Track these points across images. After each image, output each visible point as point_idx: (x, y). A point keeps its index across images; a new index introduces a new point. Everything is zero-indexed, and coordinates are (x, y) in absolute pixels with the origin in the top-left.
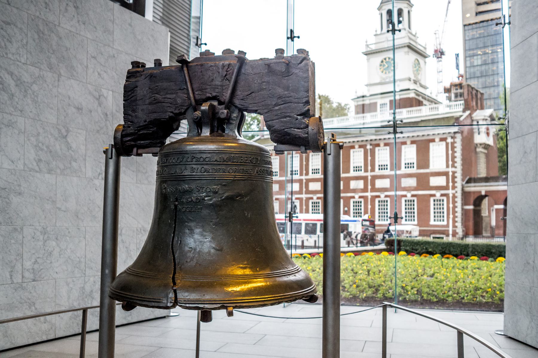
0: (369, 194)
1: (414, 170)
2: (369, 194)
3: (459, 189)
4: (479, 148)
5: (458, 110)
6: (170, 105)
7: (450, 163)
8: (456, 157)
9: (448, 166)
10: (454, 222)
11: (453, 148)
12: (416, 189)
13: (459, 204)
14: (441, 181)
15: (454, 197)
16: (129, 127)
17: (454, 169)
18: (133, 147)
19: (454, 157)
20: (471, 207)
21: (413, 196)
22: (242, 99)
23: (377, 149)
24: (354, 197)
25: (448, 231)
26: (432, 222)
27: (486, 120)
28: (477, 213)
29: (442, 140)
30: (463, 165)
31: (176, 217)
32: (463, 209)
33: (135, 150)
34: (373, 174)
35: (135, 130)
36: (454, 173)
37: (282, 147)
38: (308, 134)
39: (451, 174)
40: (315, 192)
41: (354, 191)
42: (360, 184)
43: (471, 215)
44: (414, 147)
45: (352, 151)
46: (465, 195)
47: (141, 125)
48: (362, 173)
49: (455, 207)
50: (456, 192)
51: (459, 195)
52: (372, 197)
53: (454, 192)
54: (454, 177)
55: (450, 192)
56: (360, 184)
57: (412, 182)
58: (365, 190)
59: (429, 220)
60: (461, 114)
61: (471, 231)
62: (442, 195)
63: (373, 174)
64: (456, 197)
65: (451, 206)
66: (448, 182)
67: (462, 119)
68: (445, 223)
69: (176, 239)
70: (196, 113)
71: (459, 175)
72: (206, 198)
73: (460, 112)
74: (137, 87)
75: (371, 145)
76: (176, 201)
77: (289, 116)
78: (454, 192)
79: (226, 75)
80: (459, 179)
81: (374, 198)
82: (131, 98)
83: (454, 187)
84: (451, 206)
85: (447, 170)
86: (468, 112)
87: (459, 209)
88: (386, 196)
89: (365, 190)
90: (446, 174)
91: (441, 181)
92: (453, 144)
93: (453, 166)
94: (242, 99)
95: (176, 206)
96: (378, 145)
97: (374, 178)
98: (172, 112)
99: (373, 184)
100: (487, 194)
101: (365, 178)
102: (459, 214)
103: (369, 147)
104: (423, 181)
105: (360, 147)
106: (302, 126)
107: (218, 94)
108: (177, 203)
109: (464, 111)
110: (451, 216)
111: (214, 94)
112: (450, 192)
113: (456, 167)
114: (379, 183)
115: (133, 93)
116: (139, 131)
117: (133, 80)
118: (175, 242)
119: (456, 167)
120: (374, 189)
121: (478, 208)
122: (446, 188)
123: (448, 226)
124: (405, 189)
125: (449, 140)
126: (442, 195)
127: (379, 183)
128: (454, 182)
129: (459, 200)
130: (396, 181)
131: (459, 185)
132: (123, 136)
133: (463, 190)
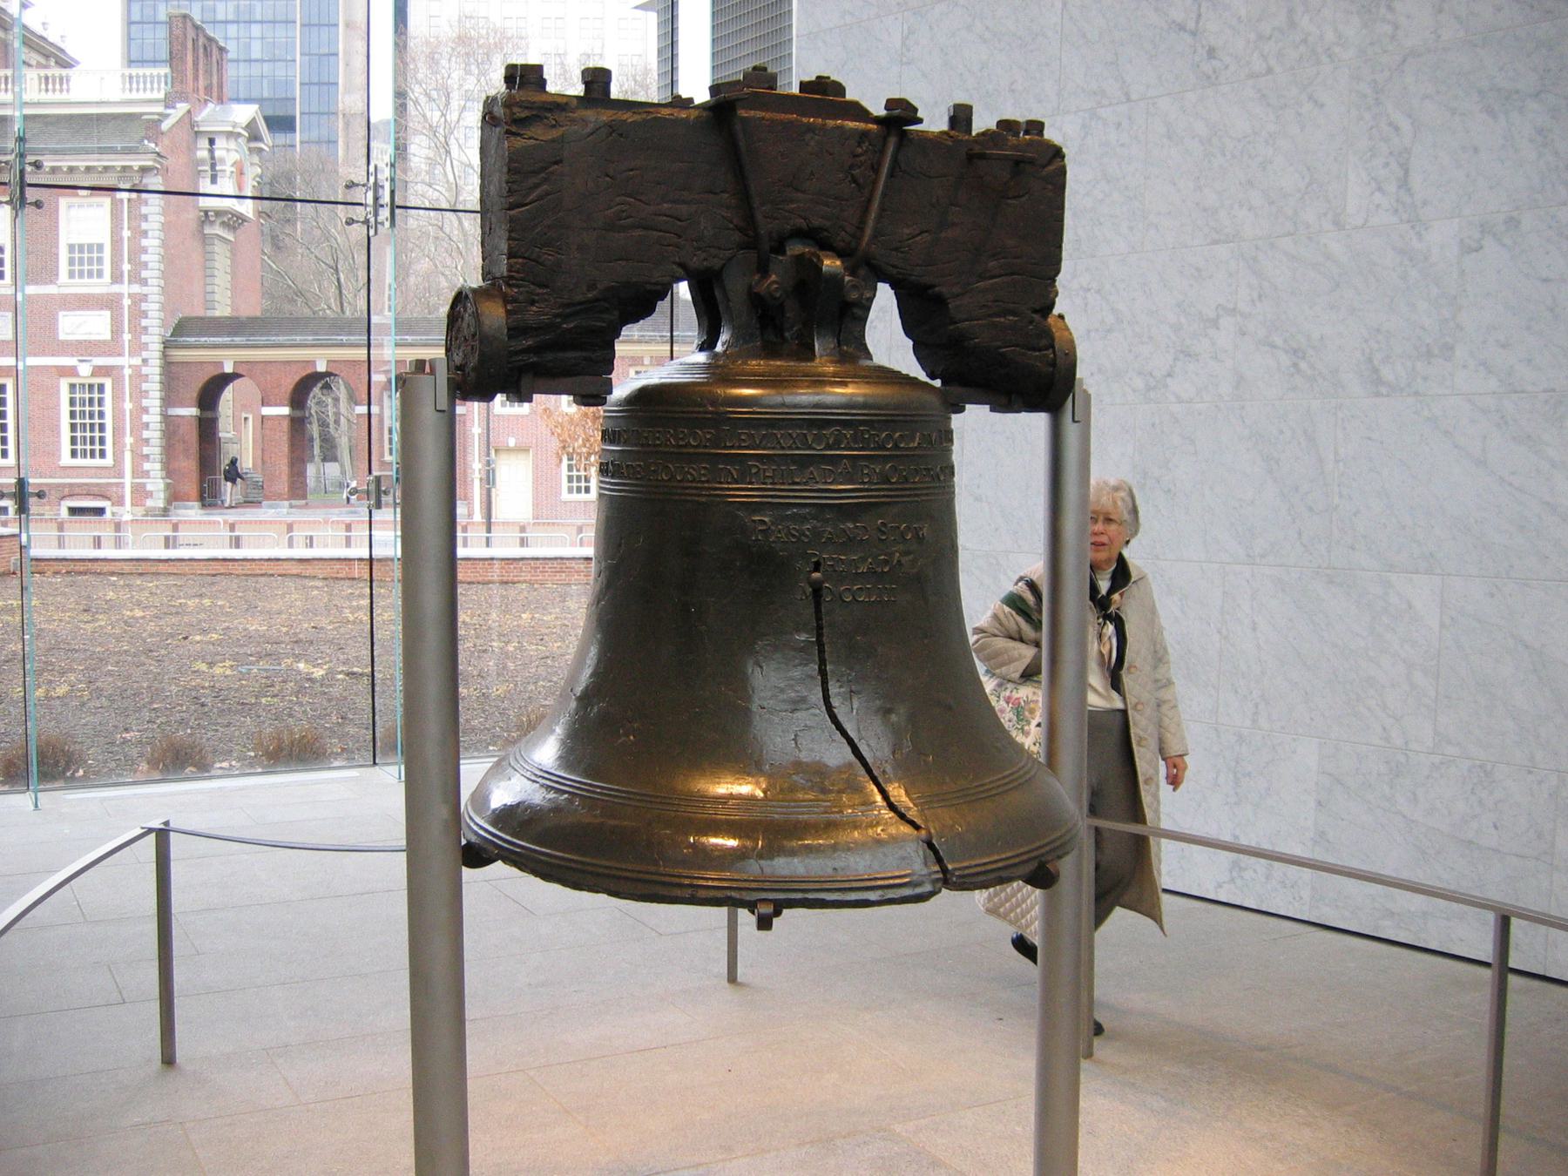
4: (212, 223)
5: (149, 95)
6: (676, 240)
7: (126, 267)
8: (145, 250)
9: (117, 278)
10: (139, 457)
13: (154, 402)
14: (96, 325)
15: (139, 377)
16: (533, 303)
17: (136, 289)
18: (522, 370)
19: (137, 251)
20: (193, 411)
22: (896, 249)
25: (121, 485)
27: (239, 135)
28: (207, 428)
30: (164, 275)
31: (819, 619)
32: (166, 418)
33: (526, 381)
35: (556, 316)
36: (138, 299)
37: (956, 390)
38: (1054, 364)
39: (127, 302)
43: (192, 436)
46: (171, 373)
47: (579, 298)
50: (145, 361)
51: (154, 370)
53: (137, 361)
54: (138, 314)
55: (125, 362)
59: (56, 453)
60: (160, 109)
61: (191, 487)
62: (98, 371)
64: (145, 378)
65: (128, 406)
66: (116, 331)
67: (165, 126)
68: (109, 461)
69: (834, 689)
70: (773, 277)
72: (904, 560)
73: (158, 101)
74: (556, 163)
76: (817, 569)
77: (1014, 313)
78: (137, 361)
79: (852, 167)
82: (540, 198)
83: (138, 348)
84: (128, 406)
85: (116, 288)
86: (182, 107)
87: (154, 418)
90: (109, 303)
91: (96, 325)
93: (136, 278)
94: (896, 249)
95: (817, 591)
98: (681, 265)
100: (240, 371)
102: (154, 434)
106: (1044, 342)
107: (828, 224)
108: (816, 575)
109: (169, 102)
110: (129, 440)
111: (817, 222)
112: (125, 362)
113: (144, 282)
115: (545, 180)
116: (566, 317)
117: (540, 133)
118: (835, 702)
119: (144, 282)
121: (209, 414)
122: (111, 347)
123: (117, 470)
128: (138, 331)
131: (154, 342)
132: (515, 331)
133: (165, 356)
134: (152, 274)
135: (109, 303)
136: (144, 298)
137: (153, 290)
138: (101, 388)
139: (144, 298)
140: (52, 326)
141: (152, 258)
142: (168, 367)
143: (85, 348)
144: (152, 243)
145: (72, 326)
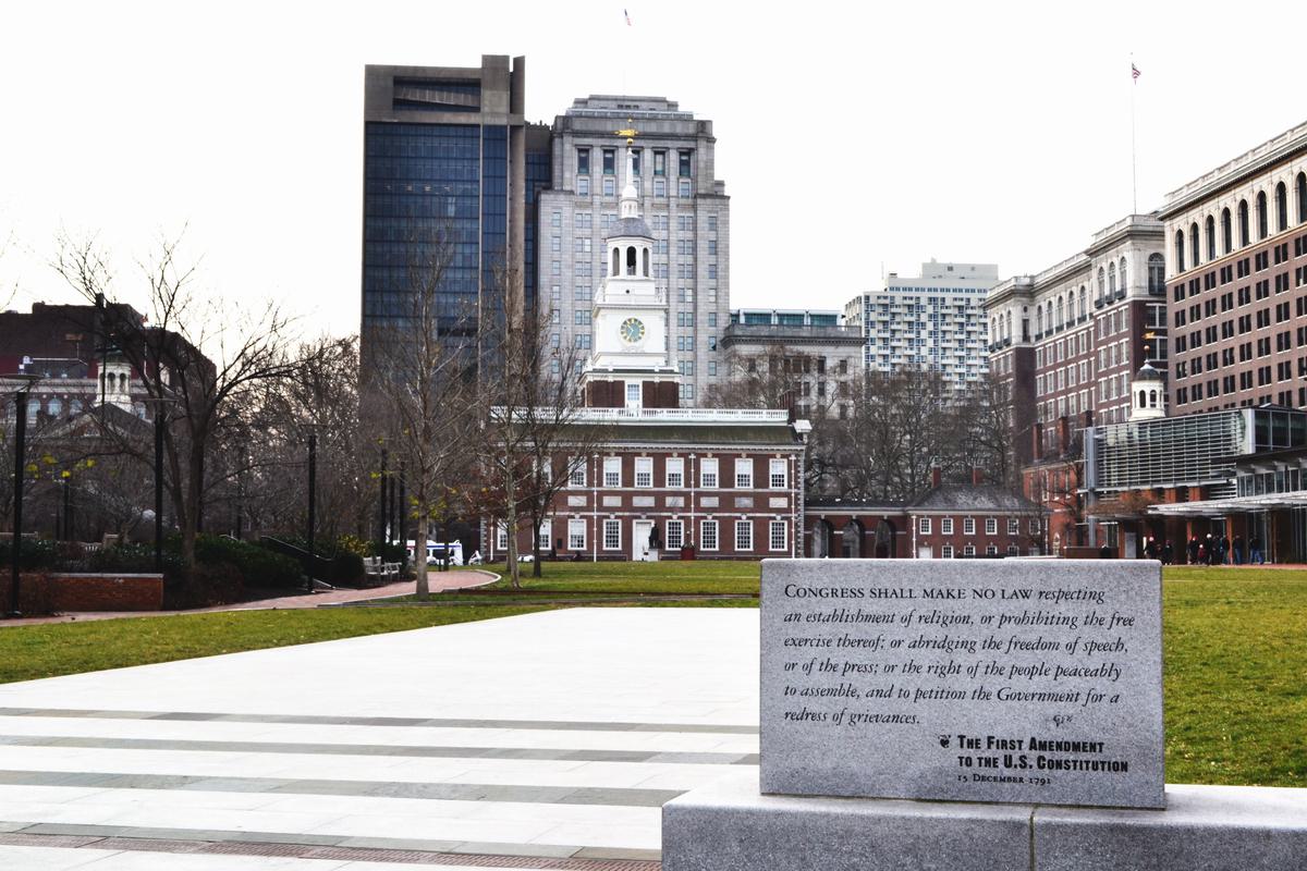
0: (692, 515)
2: (692, 515)
3: (802, 513)
9: (790, 486)
11: (797, 467)
12: (752, 511)
13: (801, 529)
19: (797, 477)
21: (748, 518)
23: (702, 459)
24: (671, 518)
29: (783, 456)
34: (697, 489)
36: (797, 494)
40: (612, 509)
41: (671, 509)
42: (681, 502)
48: (682, 487)
49: (797, 532)
51: (802, 518)
54: (797, 499)
56: (681, 502)
57: (747, 502)
58: (687, 508)
63: (697, 489)
66: (790, 504)
68: (786, 549)
71: (802, 497)
75: (695, 454)
80: (801, 502)
81: (698, 519)
83: (797, 511)
84: (793, 530)
87: (801, 535)
89: (687, 508)
91: (782, 503)
92: (796, 461)
96: (705, 456)
97: (699, 495)
99: (697, 503)
101: (687, 495)
102: (801, 540)
103: (692, 457)
104: (761, 502)
105: (680, 455)
114: (705, 502)
122: (788, 510)
125: (793, 458)
127: (705, 502)
128: (797, 505)
129: (802, 524)
130: (727, 501)
131: (802, 508)
136: (799, 494)
137: (802, 491)
138: (783, 524)
139: (799, 494)
143: (779, 511)
145: (775, 503)
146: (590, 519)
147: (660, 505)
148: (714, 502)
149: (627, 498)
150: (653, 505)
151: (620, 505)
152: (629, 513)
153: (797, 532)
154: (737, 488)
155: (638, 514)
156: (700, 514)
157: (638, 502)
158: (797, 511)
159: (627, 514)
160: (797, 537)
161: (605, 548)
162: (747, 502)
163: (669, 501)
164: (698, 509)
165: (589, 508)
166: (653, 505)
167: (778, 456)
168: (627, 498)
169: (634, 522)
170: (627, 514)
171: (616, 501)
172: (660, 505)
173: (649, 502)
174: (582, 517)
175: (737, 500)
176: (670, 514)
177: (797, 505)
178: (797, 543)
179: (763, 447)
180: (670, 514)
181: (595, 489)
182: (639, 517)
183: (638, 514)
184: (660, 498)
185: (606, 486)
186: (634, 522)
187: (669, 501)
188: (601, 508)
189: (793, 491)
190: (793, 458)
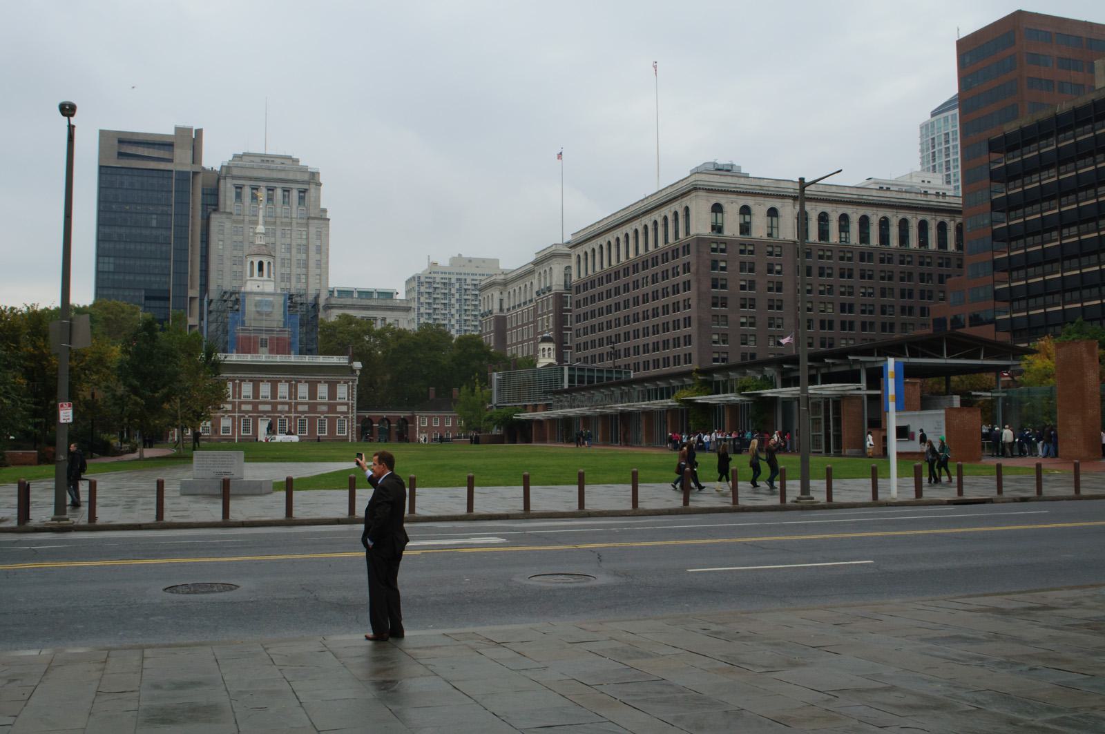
0: (293, 415)
1: (326, 400)
2: (293, 415)
3: (355, 414)
9: (348, 399)
10: (352, 434)
11: (353, 388)
13: (355, 423)
14: (344, 408)
15: (352, 418)
19: (352, 394)
21: (325, 417)
26: (337, 434)
29: (345, 383)
36: (352, 404)
41: (281, 412)
42: (286, 408)
44: (326, 386)
45: (279, 384)
51: (355, 417)
52: (295, 417)
54: (352, 407)
55: (350, 416)
56: (286, 408)
57: (325, 408)
58: (289, 411)
66: (348, 409)
71: (355, 405)
80: (355, 408)
81: (296, 418)
87: (355, 426)
88: (305, 417)
89: (289, 411)
90: (347, 404)
91: (344, 408)
92: (353, 385)
93: (352, 400)
97: (297, 404)
99: (296, 408)
101: (289, 404)
102: (355, 429)
104: (332, 408)
112: (350, 416)
114: (300, 408)
120: (296, 412)
122: (348, 413)
123: (348, 436)
124: (319, 413)
125: (351, 383)
126: (344, 417)
127: (300, 408)
128: (352, 410)
129: (355, 420)
130: (313, 408)
131: (355, 411)
134: (355, 399)
135: (347, 404)
137: (355, 402)
140: (336, 408)
141: (355, 396)
142: (358, 417)
143: (342, 413)
144: (355, 393)
145: (340, 408)
146: (233, 418)
147: (274, 410)
148: (306, 408)
149: (255, 405)
150: (270, 410)
151: (251, 409)
152: (257, 414)
153: (352, 425)
154: (319, 400)
155: (262, 415)
156: (297, 415)
157: (261, 408)
158: (352, 413)
159: (255, 414)
160: (352, 428)
161: (242, 434)
162: (325, 408)
163: (280, 408)
164: (296, 412)
165: (233, 411)
166: (270, 410)
167: (342, 382)
168: (255, 405)
169: (259, 419)
170: (255, 414)
171: (249, 407)
172: (274, 410)
173: (268, 408)
174: (229, 416)
175: (318, 407)
176: (279, 415)
177: (352, 410)
178: (352, 431)
179: (334, 378)
180: (279, 415)
181: (237, 400)
182: (262, 417)
183: (262, 415)
184: (274, 405)
185: (243, 399)
186: (259, 419)
187: (280, 408)
188: (240, 411)
189: (350, 402)
190: (351, 383)
